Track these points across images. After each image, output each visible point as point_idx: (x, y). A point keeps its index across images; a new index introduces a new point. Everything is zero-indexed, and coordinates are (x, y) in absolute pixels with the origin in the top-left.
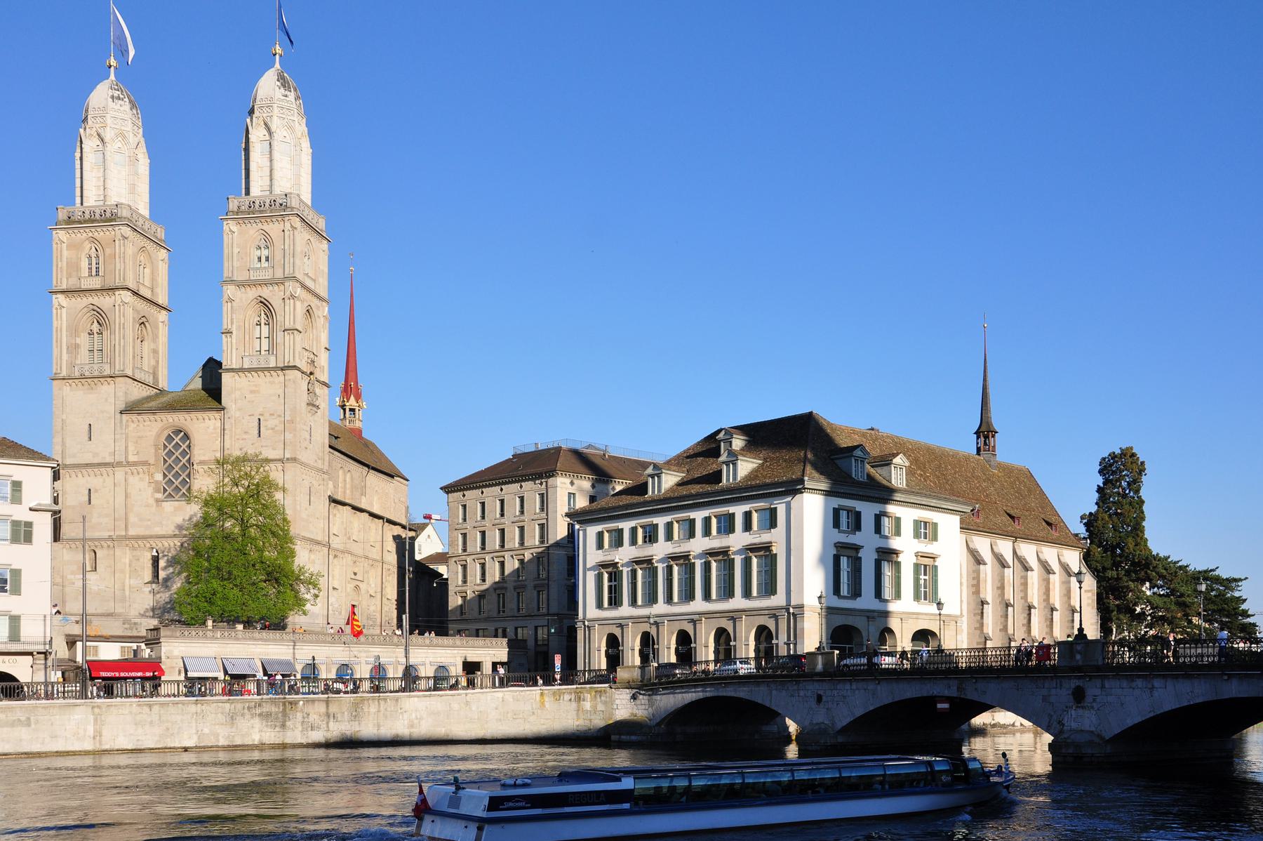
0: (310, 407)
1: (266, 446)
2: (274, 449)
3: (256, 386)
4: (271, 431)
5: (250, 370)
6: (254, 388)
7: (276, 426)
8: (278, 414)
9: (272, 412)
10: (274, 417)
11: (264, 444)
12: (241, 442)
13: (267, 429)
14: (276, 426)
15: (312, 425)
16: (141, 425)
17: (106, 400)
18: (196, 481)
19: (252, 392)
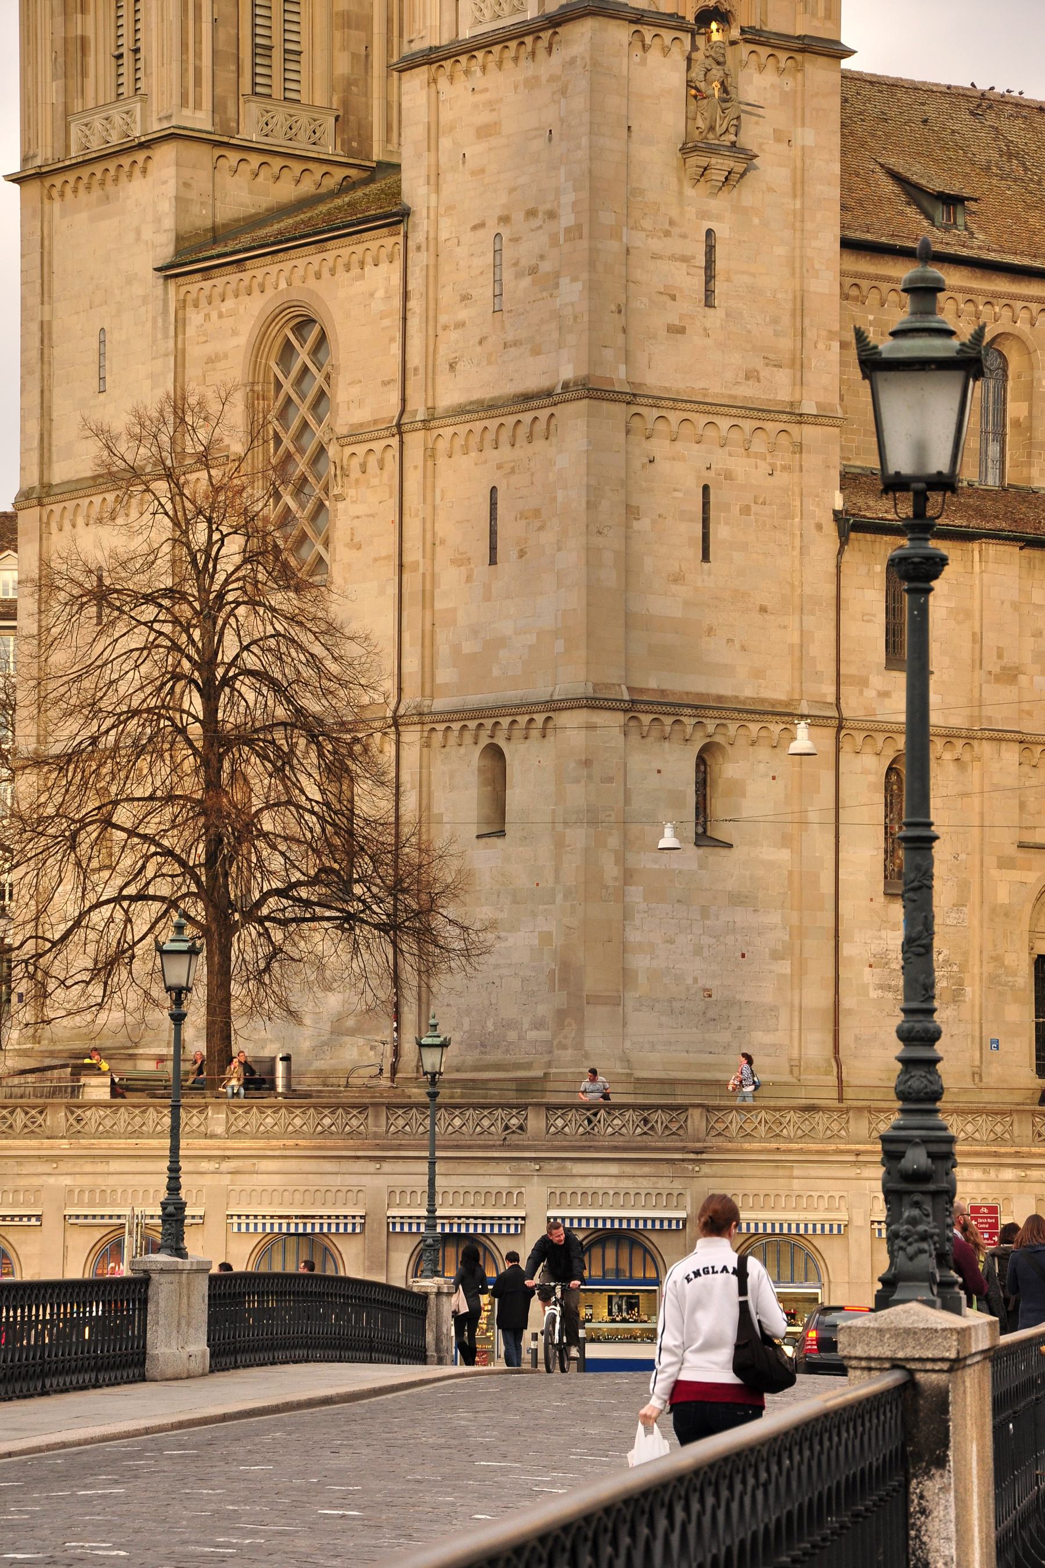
0: (697, 160)
1: (516, 344)
2: (536, 352)
3: (491, 105)
4: (526, 281)
5: (470, 49)
6: (485, 117)
7: (542, 257)
8: (548, 206)
9: (531, 205)
10: (535, 223)
11: (510, 337)
12: (454, 335)
13: (519, 276)
14: (542, 257)
15: (722, 231)
16: (214, 315)
17: (138, 232)
18: (340, 505)
19: (484, 132)
